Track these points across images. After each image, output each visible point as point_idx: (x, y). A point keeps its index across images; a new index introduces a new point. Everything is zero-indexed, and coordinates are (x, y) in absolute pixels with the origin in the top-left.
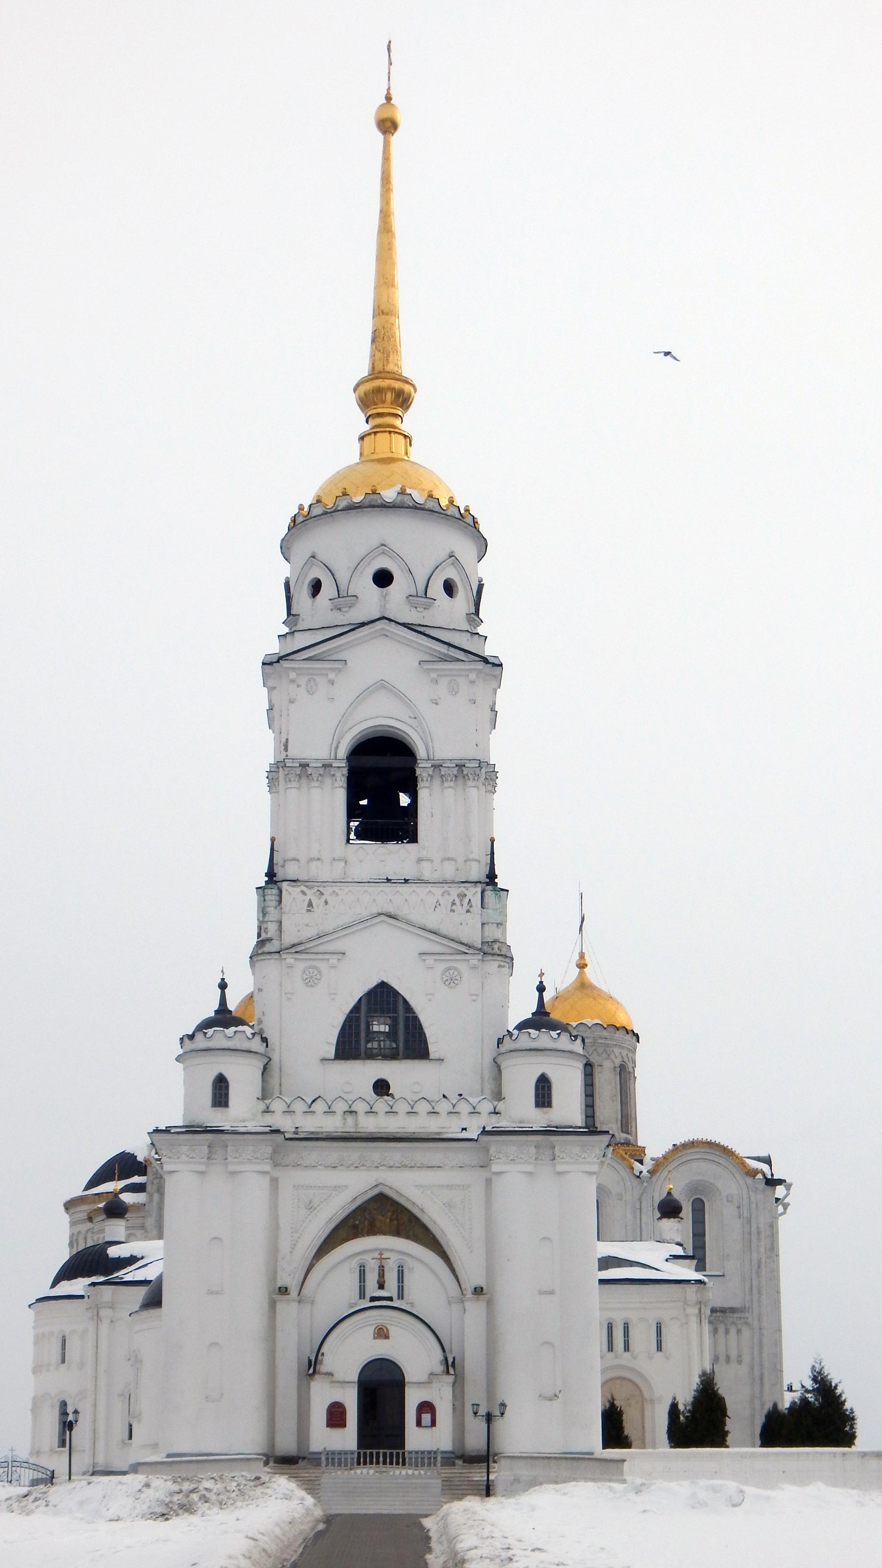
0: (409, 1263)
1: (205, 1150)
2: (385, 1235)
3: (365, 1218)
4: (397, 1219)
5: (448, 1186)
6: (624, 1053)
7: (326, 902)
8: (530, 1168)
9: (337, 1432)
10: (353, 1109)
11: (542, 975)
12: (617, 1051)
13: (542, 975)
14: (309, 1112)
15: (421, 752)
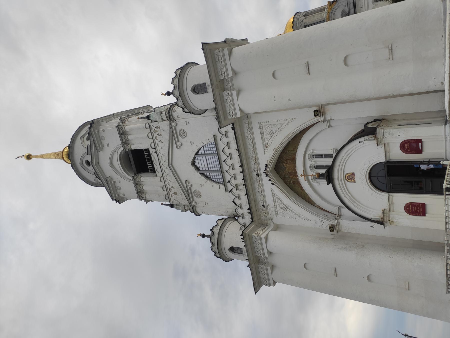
0: (309, 152)
1: (260, 266)
2: (295, 167)
3: (288, 177)
4: (286, 160)
5: (262, 136)
6: (301, 16)
7: (172, 187)
8: (234, 93)
9: (429, 209)
10: (235, 186)
11: (162, 94)
12: (300, 19)
13: (162, 94)
14: (241, 206)
15: (122, 149)
